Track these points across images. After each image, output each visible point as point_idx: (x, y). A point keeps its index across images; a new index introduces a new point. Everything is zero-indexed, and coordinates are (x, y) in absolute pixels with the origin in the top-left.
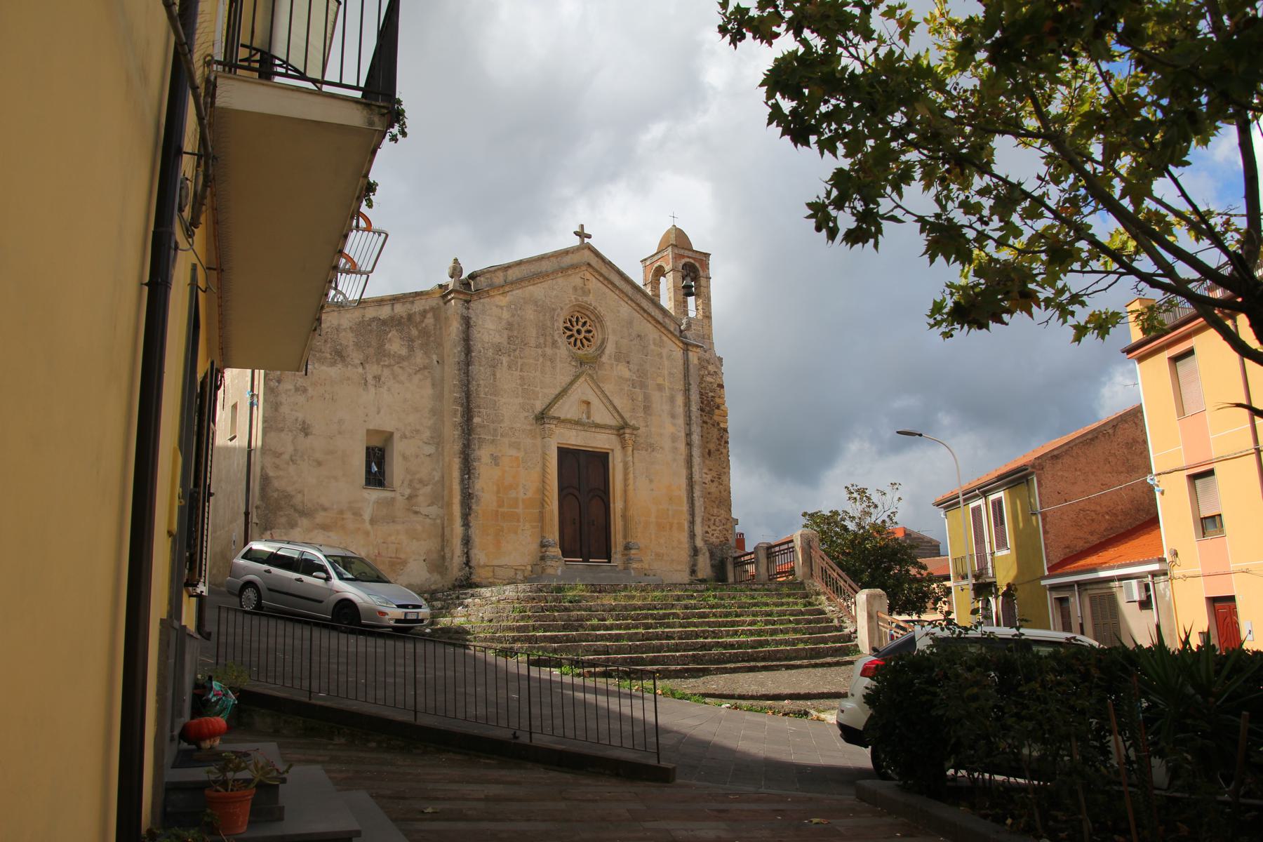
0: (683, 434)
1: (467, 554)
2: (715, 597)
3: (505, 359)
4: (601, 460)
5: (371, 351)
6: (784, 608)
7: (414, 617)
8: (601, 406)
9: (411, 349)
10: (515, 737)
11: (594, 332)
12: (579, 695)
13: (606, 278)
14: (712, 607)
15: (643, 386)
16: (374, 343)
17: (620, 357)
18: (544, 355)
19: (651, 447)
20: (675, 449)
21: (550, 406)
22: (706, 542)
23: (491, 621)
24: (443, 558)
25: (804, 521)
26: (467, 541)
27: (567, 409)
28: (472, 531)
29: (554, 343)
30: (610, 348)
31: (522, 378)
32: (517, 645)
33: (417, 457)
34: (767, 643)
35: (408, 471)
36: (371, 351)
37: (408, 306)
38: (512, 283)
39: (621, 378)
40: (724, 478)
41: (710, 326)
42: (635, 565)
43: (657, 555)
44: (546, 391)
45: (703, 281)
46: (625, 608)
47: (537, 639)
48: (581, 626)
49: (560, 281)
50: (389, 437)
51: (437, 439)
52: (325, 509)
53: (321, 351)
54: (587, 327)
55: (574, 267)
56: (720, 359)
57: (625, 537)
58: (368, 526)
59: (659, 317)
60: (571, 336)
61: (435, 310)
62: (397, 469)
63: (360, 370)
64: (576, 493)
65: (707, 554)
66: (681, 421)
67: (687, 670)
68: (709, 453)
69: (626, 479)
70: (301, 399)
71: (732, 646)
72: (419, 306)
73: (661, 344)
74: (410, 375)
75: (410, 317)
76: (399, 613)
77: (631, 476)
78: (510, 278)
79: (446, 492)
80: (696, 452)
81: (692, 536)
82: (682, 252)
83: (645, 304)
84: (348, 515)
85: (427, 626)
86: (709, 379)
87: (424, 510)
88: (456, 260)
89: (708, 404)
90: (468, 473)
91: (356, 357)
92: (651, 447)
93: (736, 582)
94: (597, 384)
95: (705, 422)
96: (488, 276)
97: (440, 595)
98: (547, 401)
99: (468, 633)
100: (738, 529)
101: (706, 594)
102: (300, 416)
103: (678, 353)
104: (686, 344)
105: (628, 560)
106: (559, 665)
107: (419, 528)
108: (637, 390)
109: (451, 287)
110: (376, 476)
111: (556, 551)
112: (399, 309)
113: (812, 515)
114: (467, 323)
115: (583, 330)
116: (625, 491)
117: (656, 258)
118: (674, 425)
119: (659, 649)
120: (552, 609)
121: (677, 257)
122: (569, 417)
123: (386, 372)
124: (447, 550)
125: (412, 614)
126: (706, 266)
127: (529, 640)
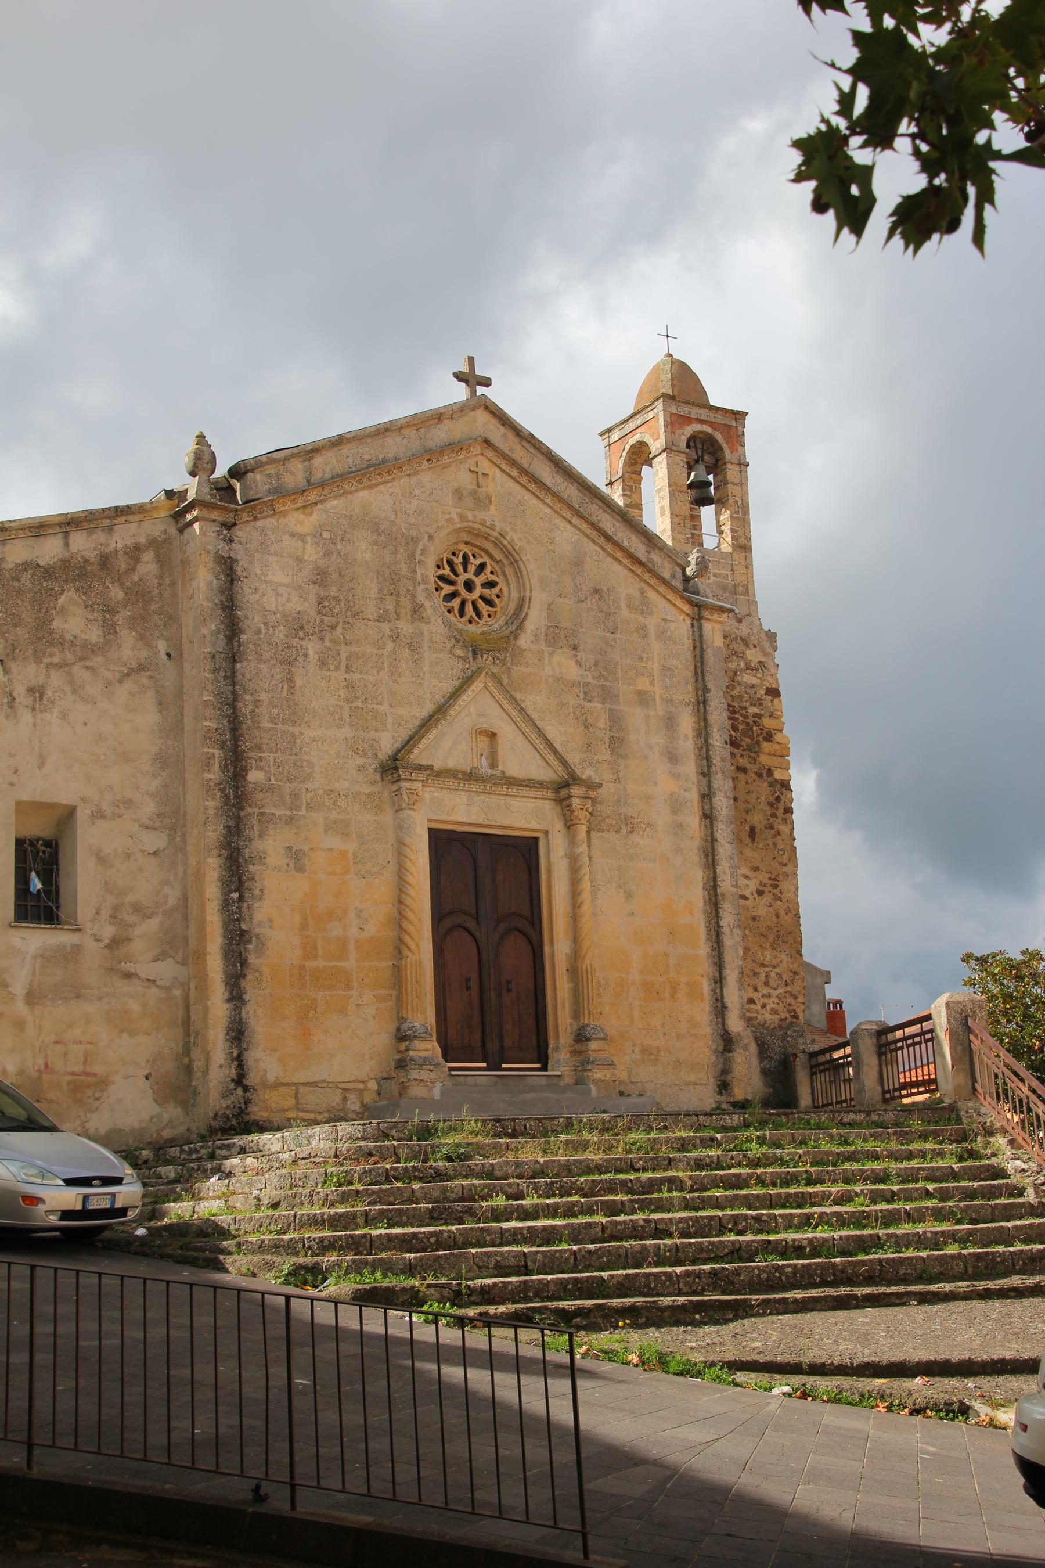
0: (694, 796)
1: (239, 1061)
2: (761, 1141)
3: (312, 647)
4: (524, 852)
6: (914, 1164)
7: (105, 1204)
8: (520, 739)
9: (110, 629)
10: (259, 1497)
11: (502, 584)
12: (453, 1373)
13: (524, 472)
14: (755, 1163)
15: (608, 696)
18: (396, 637)
19: (629, 825)
21: (411, 741)
22: (749, 1021)
23: (275, 1206)
24: (188, 1070)
25: (966, 971)
26: (238, 1033)
27: (449, 747)
29: (417, 611)
30: (535, 619)
31: (350, 685)
32: (332, 1257)
33: (128, 856)
34: (876, 1243)
35: (108, 887)
36: (22, 634)
37: (101, 537)
38: (322, 485)
39: (559, 679)
40: (784, 885)
41: (748, 567)
42: (598, 1074)
43: (645, 1050)
44: (401, 711)
45: (732, 473)
46: (568, 1169)
47: (372, 1245)
48: (470, 1212)
49: (427, 478)
50: (67, 816)
51: (172, 820)
54: (487, 576)
55: (455, 447)
56: (772, 637)
57: (576, 1014)
58: (21, 1008)
59: (639, 548)
60: (453, 595)
61: (160, 546)
62: (85, 884)
64: (471, 924)
65: (753, 1048)
66: (690, 768)
67: (698, 1307)
68: (752, 833)
69: (575, 893)
71: (798, 1250)
72: (123, 537)
73: (643, 607)
74: (108, 684)
75: (105, 561)
76: (71, 1198)
77: (586, 884)
78: (318, 475)
79: (192, 930)
80: (724, 832)
81: (720, 1009)
82: (685, 410)
83: (609, 523)
85: (139, 1221)
86: (748, 678)
87: (146, 969)
88: (201, 438)
89: (748, 732)
90: (240, 888)
92: (629, 825)
93: (816, 1107)
94: (508, 693)
96: (271, 470)
97: (174, 1151)
98: (404, 734)
99: (224, 1233)
100: (831, 992)
101: (743, 1135)
103: (681, 626)
104: (698, 606)
105: (583, 1064)
106: (413, 1301)
107: (135, 1007)
108: (596, 705)
109: (191, 496)
111: (429, 1048)
112: (82, 544)
113: (982, 960)
114: (229, 571)
115: (478, 581)
116: (575, 919)
117: (631, 426)
118: (676, 776)
119: (638, 1259)
120: (409, 1176)
121: (674, 422)
122: (451, 764)
123: (57, 679)
124: (196, 1053)
125: (100, 1197)
126: (737, 438)
127: (355, 1245)
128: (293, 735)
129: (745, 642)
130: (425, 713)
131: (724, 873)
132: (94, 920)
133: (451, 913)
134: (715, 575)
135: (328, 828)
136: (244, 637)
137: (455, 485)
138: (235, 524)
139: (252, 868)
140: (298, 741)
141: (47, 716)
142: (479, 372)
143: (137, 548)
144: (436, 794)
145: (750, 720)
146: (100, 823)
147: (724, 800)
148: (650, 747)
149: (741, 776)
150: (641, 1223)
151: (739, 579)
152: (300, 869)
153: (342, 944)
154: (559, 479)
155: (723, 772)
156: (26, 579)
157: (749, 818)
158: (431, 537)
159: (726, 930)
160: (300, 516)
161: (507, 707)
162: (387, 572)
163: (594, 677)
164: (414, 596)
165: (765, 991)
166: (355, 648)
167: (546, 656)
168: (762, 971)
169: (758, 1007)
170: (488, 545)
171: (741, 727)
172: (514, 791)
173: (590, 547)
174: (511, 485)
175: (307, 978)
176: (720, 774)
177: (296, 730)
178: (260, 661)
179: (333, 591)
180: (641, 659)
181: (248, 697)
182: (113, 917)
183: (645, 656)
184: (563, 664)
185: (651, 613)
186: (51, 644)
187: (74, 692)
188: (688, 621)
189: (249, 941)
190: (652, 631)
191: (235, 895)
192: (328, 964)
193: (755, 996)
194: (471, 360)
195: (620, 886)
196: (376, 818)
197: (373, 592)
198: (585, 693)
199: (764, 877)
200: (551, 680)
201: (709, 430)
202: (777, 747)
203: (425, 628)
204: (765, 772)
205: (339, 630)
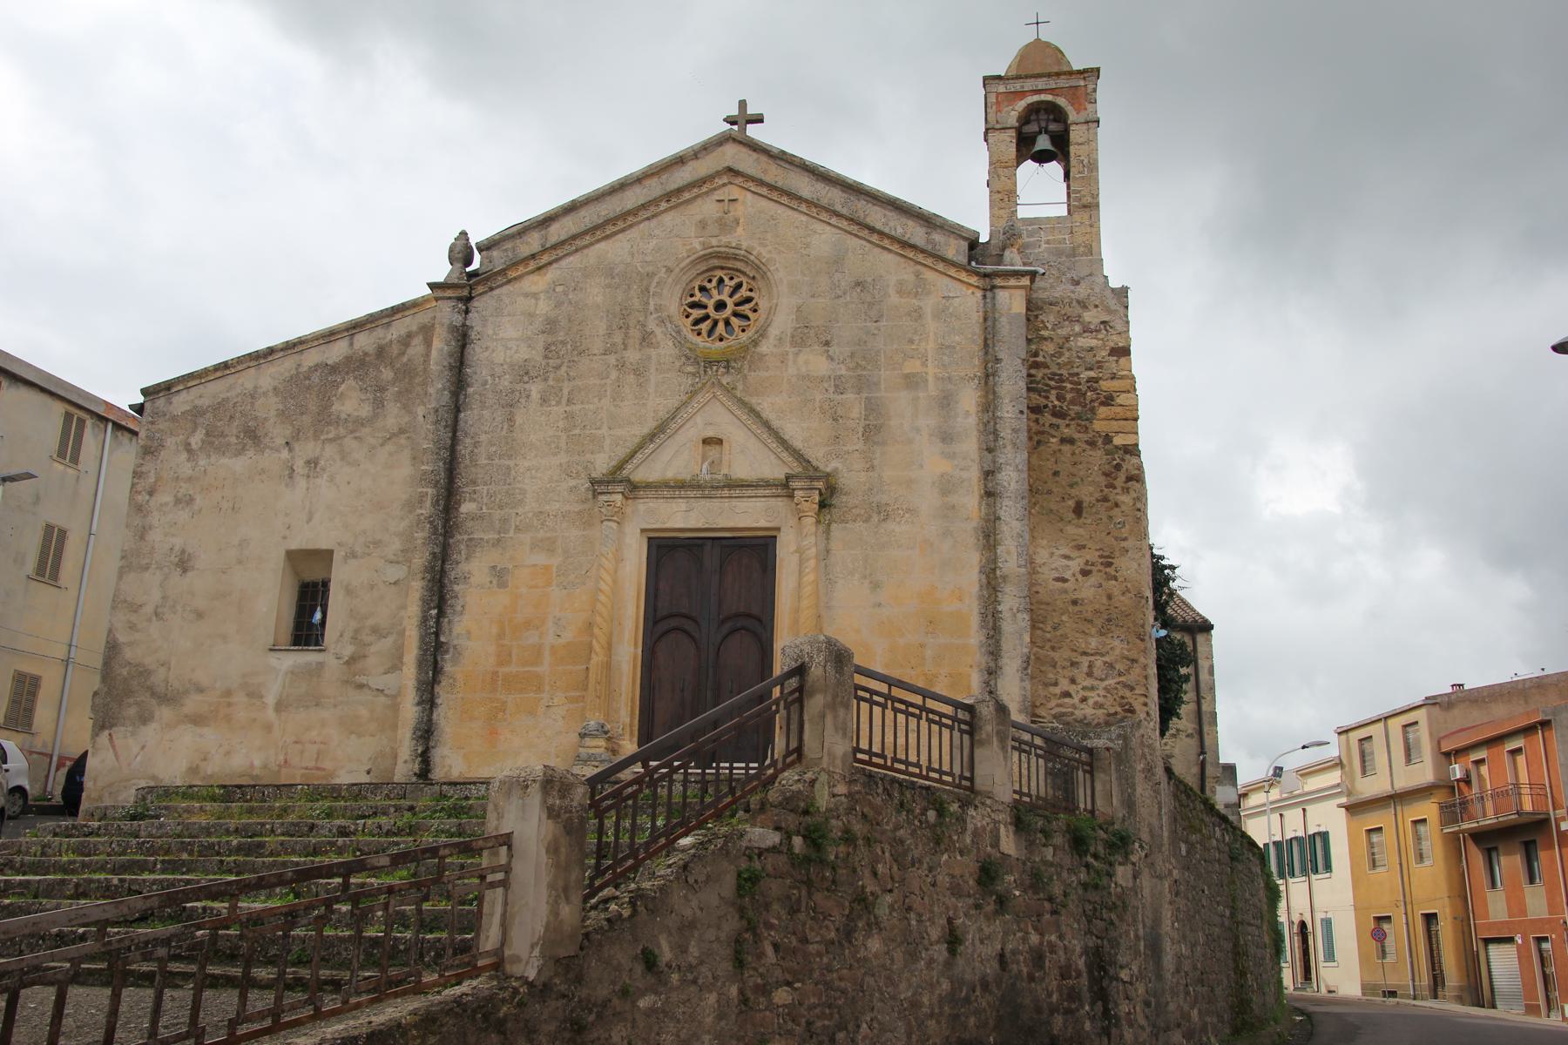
0: (974, 474)
3: (535, 389)
4: (757, 552)
5: (307, 419)
9: (379, 404)
15: (863, 384)
16: (313, 406)
17: (801, 337)
18: (621, 366)
20: (949, 511)
28: (440, 715)
29: (646, 339)
30: (782, 323)
31: (569, 416)
33: (372, 587)
36: (307, 419)
37: (380, 332)
41: (1094, 224)
44: (619, 432)
49: (667, 219)
52: (200, 690)
53: (222, 435)
54: (744, 293)
56: (1122, 293)
58: (271, 714)
62: (337, 615)
63: (285, 454)
64: (689, 625)
66: (970, 445)
68: (1078, 510)
70: (183, 515)
75: (381, 351)
78: (553, 240)
80: (1011, 513)
82: (1017, 86)
84: (240, 698)
86: (1086, 342)
87: (376, 681)
91: (278, 433)
92: (884, 512)
95: (1071, 441)
96: (509, 245)
98: (622, 452)
102: (178, 542)
107: (364, 712)
108: (850, 396)
110: (306, 633)
112: (364, 341)
114: (463, 338)
118: (951, 456)
122: (670, 474)
123: (330, 450)
128: (509, 468)
129: (1083, 305)
130: (646, 431)
131: (1008, 553)
132: (337, 641)
133: (671, 616)
134: (1048, 242)
136: (470, 390)
137: (699, 217)
138: (470, 299)
139: (456, 588)
141: (318, 481)
142: (751, 110)
143: (410, 336)
145: (1083, 388)
146: (352, 562)
147: (1014, 475)
148: (918, 430)
149: (1066, 448)
150: (115, 882)
151: (1079, 239)
152: (502, 585)
153: (538, 652)
154: (820, 186)
155: (1014, 444)
156: (316, 378)
157: (1073, 492)
158: (669, 270)
159: (1006, 615)
160: (535, 278)
161: (738, 413)
162: (618, 309)
163: (848, 369)
164: (644, 326)
165: (1088, 682)
166: (579, 383)
167: (791, 357)
168: (1085, 661)
169: (1076, 700)
170: (739, 265)
171: (1069, 396)
172: (737, 492)
173: (853, 242)
174: (764, 203)
176: (1009, 447)
177: (511, 463)
178: (483, 406)
179: (561, 336)
180: (911, 341)
181: (468, 441)
182: (354, 638)
183: (916, 338)
184: (816, 363)
185: (929, 293)
186: (329, 424)
187: (343, 459)
188: (979, 294)
189: (447, 652)
190: (928, 311)
191: (434, 612)
192: (521, 669)
193: (1072, 689)
194: (743, 104)
195: (865, 577)
197: (601, 327)
198: (836, 386)
199: (1092, 555)
200: (794, 380)
201: (1049, 98)
202: (1119, 409)
203: (653, 352)
204: (1100, 441)
205: (564, 369)
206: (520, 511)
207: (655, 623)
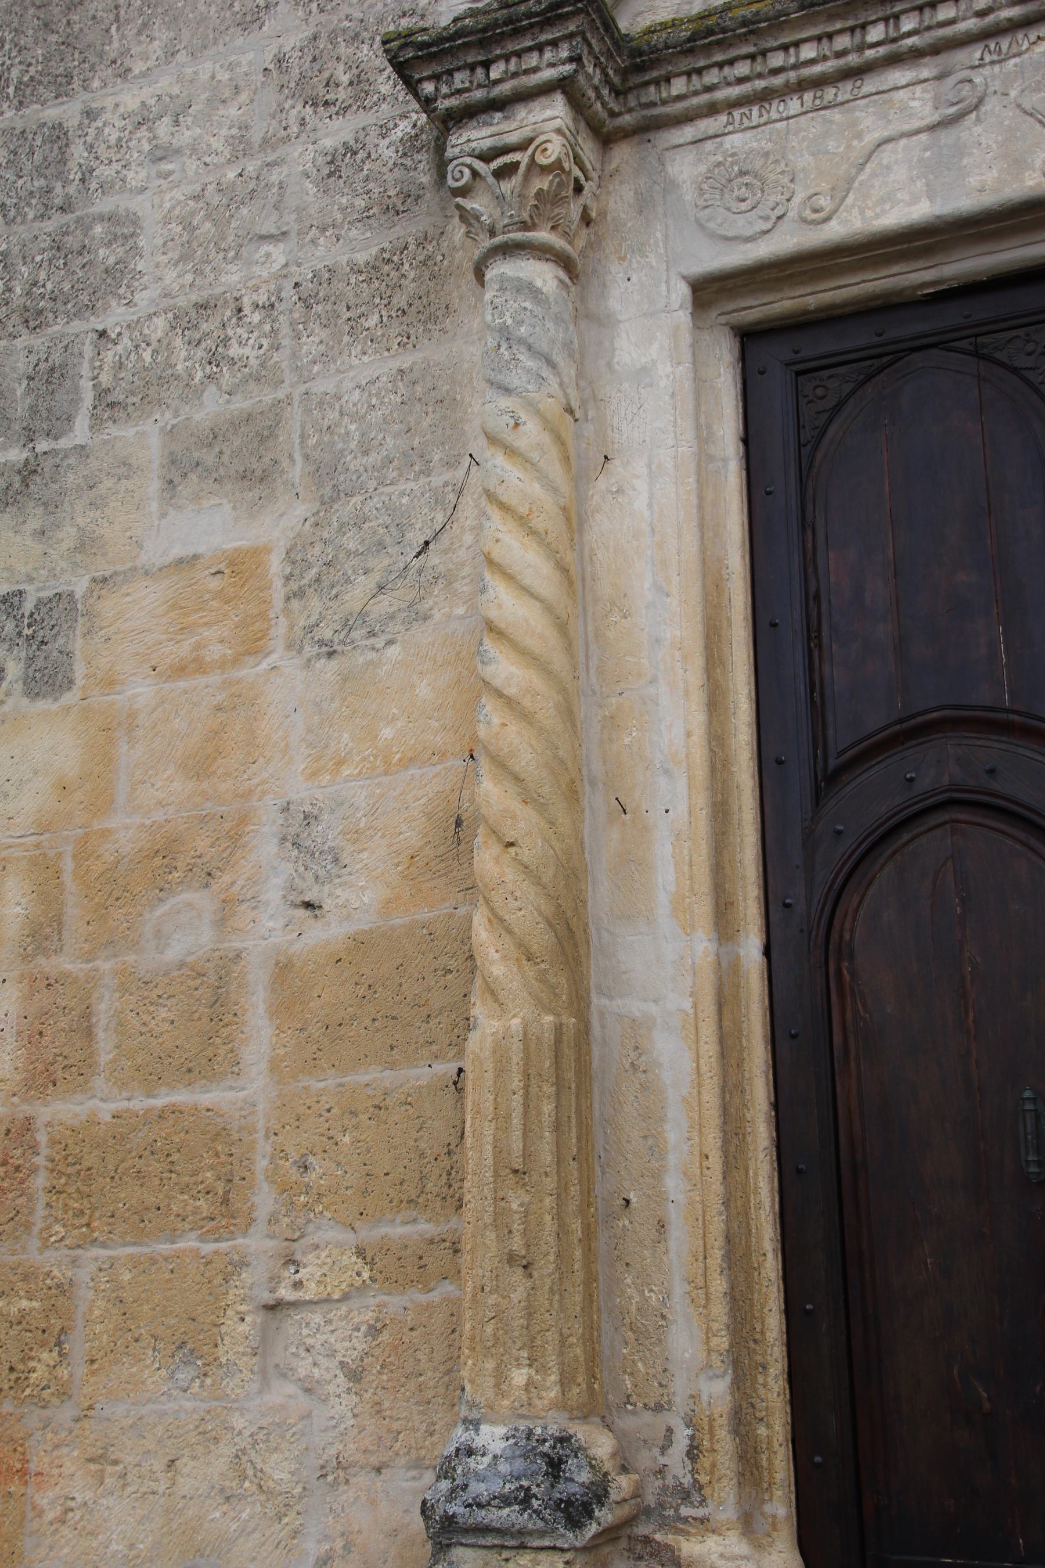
135: (178, 471)
140: (78, 152)
144: (734, 141)
153: (213, 991)
175: (40, 1181)
177: (66, 112)
192: (139, 1104)
196: (406, 360)
206: (114, 317)
207: (827, 781)
